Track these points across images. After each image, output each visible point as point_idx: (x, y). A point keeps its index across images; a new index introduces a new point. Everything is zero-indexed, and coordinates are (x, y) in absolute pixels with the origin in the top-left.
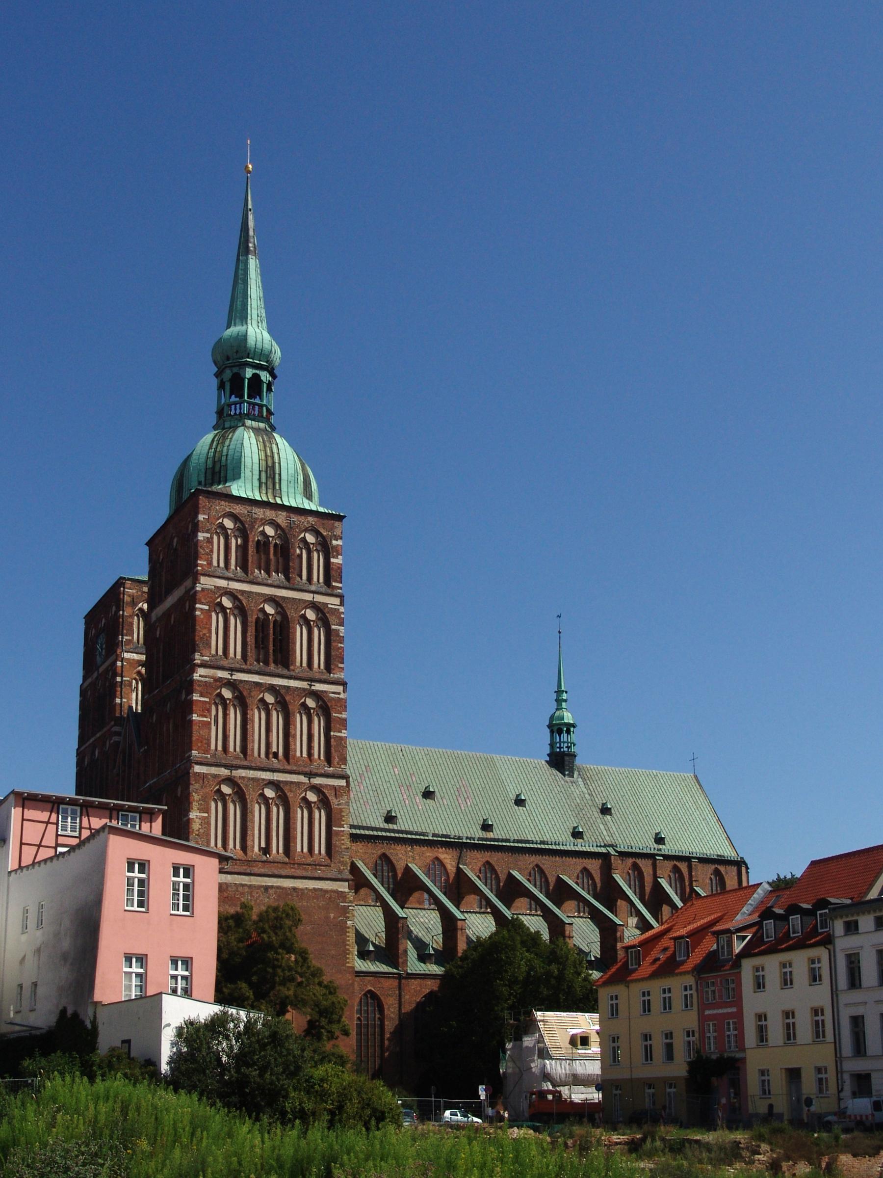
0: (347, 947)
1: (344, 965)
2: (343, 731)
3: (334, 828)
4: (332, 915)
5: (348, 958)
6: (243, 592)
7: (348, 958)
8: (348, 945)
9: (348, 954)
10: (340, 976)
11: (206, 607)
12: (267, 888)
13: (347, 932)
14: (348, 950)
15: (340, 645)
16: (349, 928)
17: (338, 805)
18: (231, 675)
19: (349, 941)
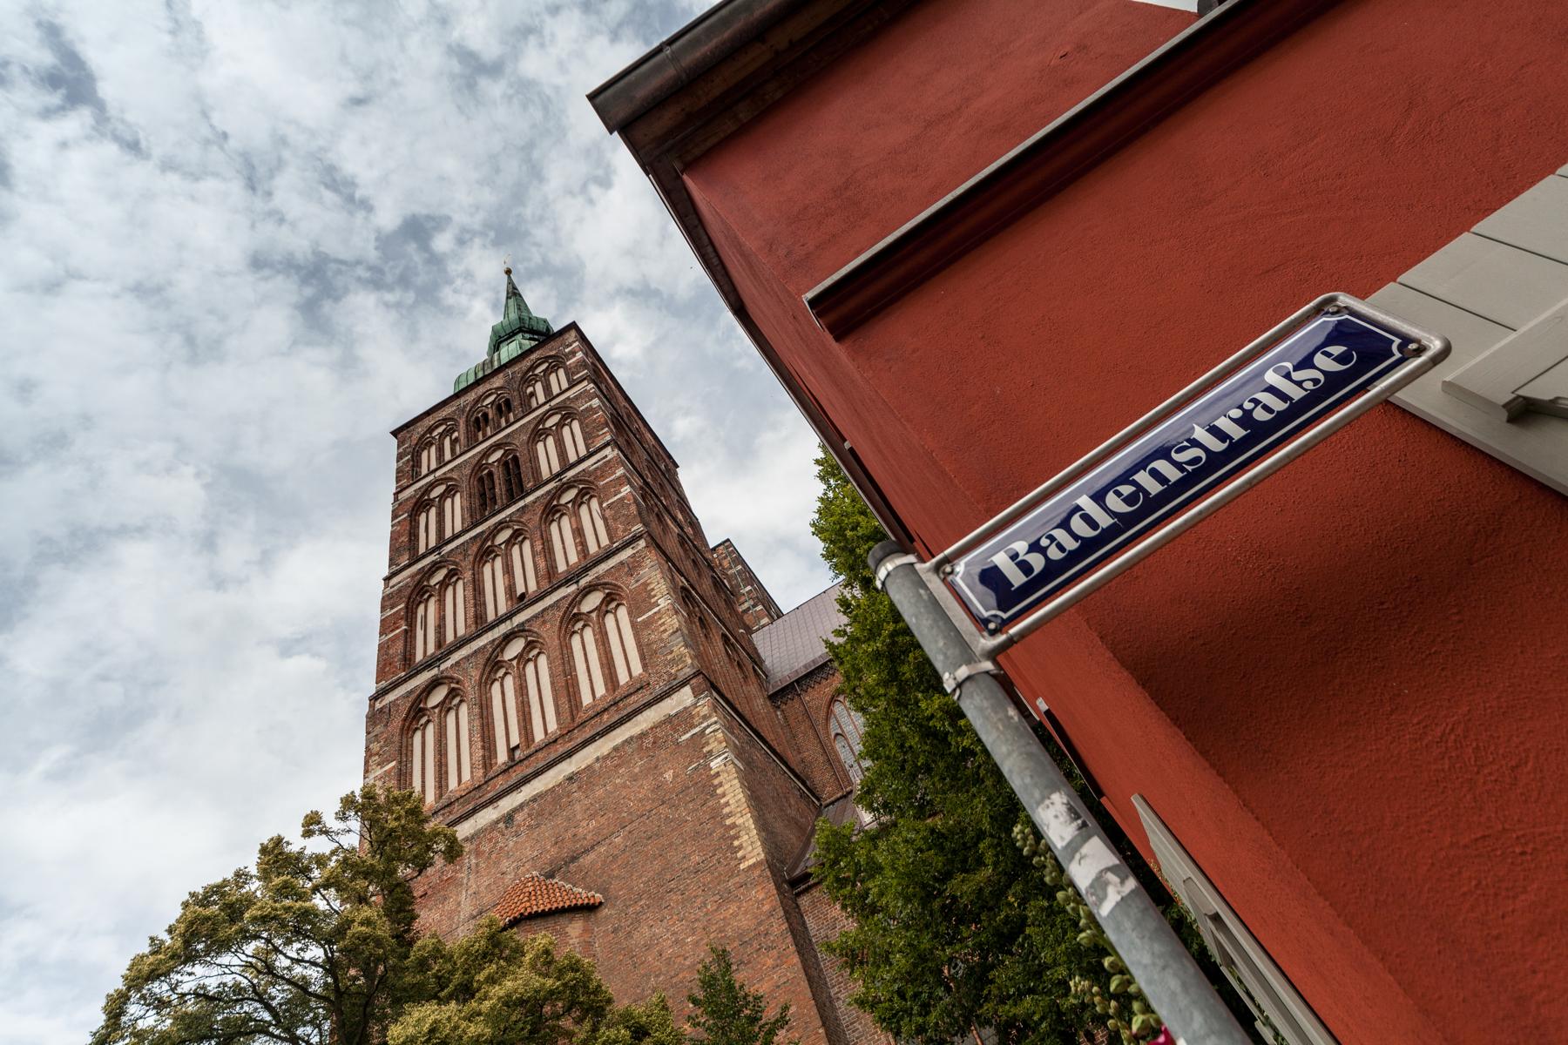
0: (728, 822)
1: (733, 872)
2: (622, 490)
3: (639, 620)
4: (669, 775)
5: (740, 847)
6: (452, 470)
7: (740, 847)
8: (729, 815)
9: (737, 837)
10: (733, 908)
11: (406, 515)
12: (509, 818)
13: (716, 787)
14: (734, 826)
15: (595, 416)
16: (718, 774)
17: (637, 581)
18: (439, 554)
19: (727, 804)
